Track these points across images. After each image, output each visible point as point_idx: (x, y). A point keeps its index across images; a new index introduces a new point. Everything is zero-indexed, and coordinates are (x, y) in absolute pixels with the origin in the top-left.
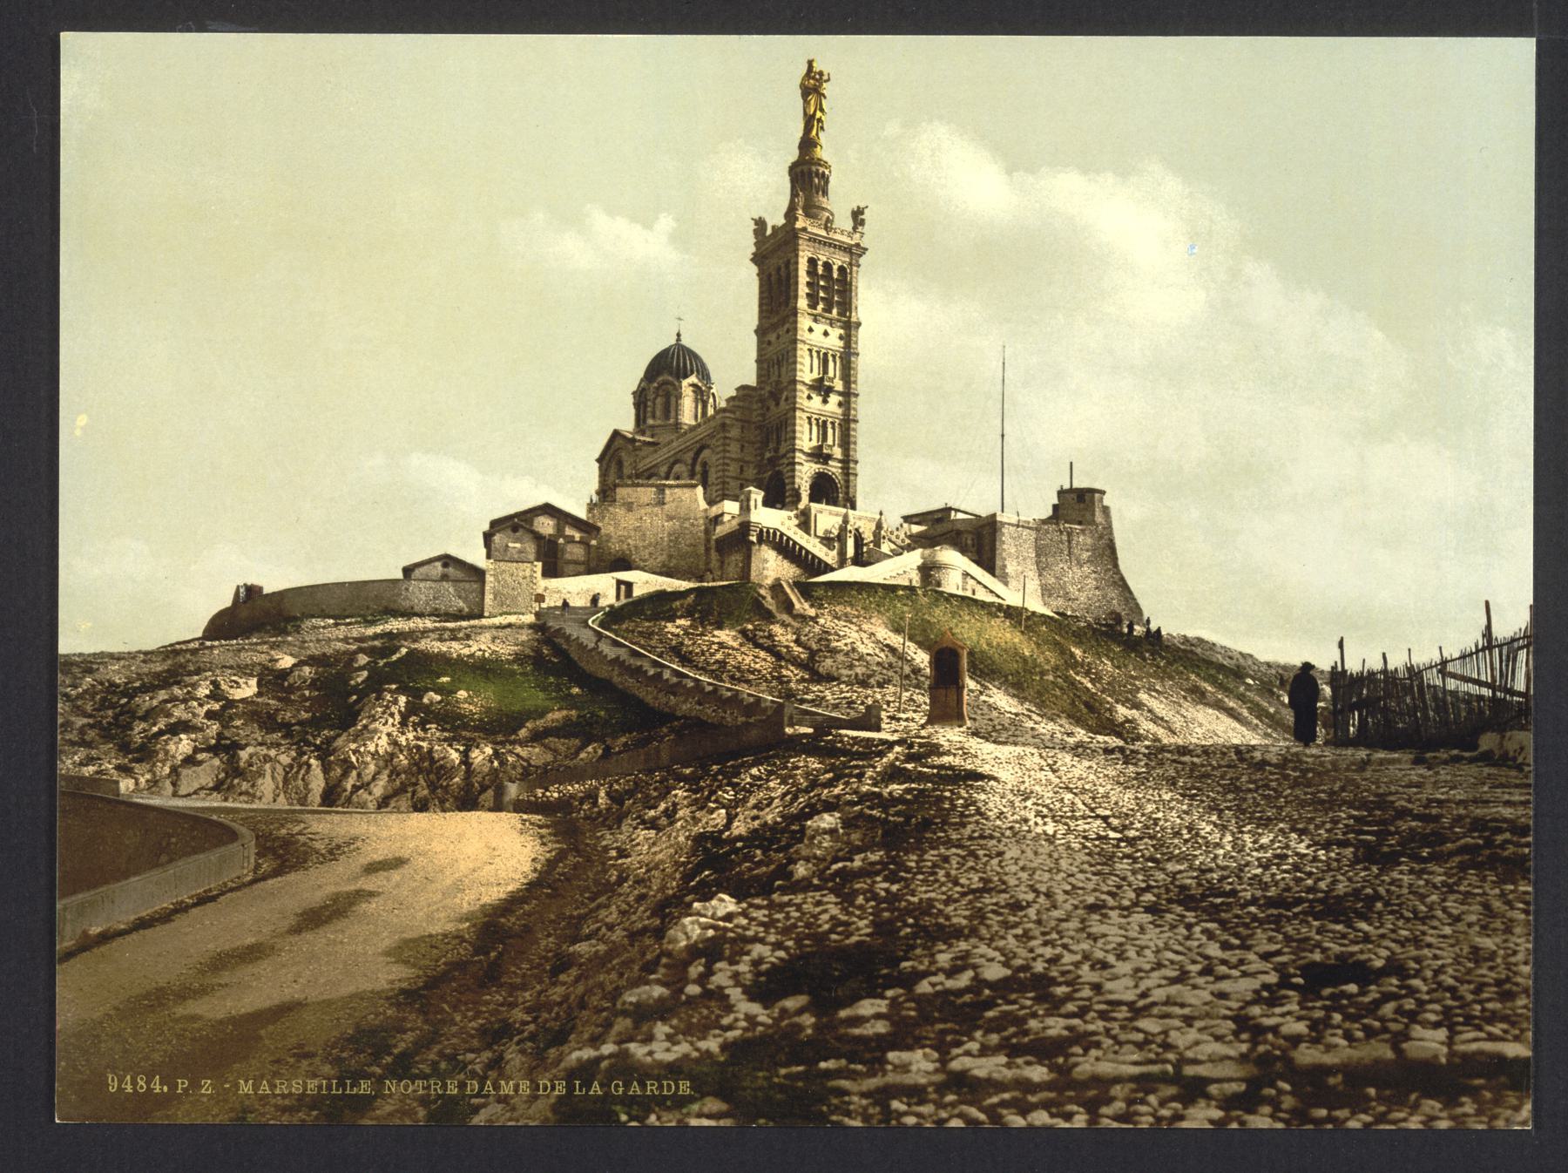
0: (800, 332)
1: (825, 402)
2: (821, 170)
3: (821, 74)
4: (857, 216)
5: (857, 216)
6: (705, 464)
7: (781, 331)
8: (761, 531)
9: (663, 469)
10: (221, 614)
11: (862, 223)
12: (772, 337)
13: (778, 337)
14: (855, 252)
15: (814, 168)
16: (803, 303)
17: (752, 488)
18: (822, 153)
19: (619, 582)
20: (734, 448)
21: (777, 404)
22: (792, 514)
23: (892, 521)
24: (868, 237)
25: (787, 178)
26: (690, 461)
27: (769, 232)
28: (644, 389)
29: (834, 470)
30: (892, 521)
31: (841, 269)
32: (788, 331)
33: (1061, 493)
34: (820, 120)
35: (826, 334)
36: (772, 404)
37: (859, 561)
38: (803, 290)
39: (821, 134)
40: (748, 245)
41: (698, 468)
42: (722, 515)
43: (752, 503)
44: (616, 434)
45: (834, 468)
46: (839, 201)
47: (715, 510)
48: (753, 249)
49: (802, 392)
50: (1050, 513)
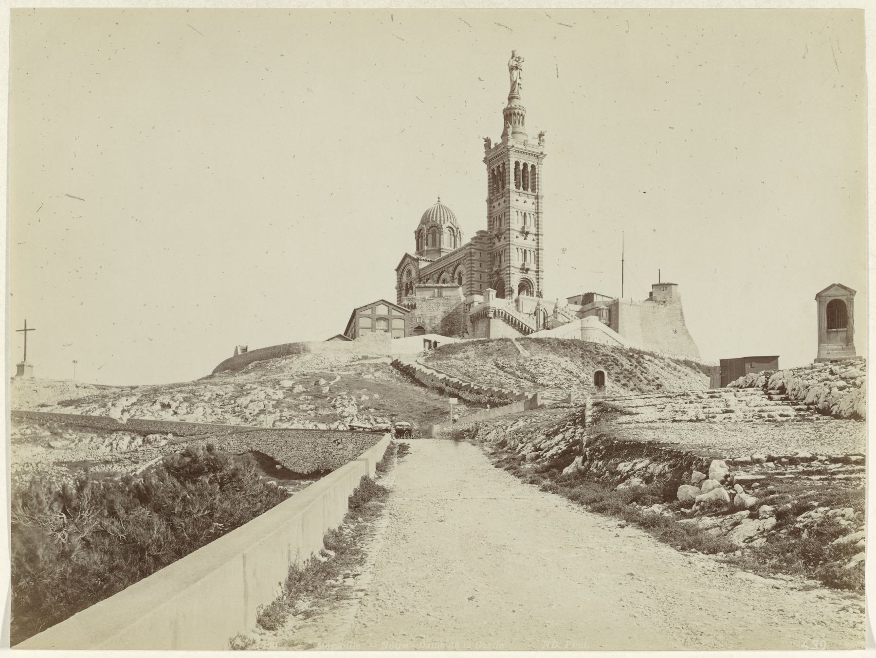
0: (511, 202)
6: (460, 274)
7: (501, 201)
8: (495, 311)
9: (435, 277)
10: (227, 361)
12: (496, 204)
13: (499, 204)
14: (539, 156)
15: (516, 111)
16: (512, 186)
17: (490, 289)
19: (425, 341)
20: (476, 265)
21: (499, 241)
22: (510, 301)
23: (563, 303)
24: (547, 148)
25: (502, 116)
26: (451, 271)
28: (421, 230)
29: (531, 276)
30: (563, 303)
31: (533, 167)
32: (505, 202)
35: (525, 202)
36: (496, 240)
37: (546, 327)
41: (456, 276)
42: (473, 302)
43: (490, 297)
44: (407, 256)
45: (531, 276)
47: (469, 300)
48: (484, 155)
49: (513, 234)
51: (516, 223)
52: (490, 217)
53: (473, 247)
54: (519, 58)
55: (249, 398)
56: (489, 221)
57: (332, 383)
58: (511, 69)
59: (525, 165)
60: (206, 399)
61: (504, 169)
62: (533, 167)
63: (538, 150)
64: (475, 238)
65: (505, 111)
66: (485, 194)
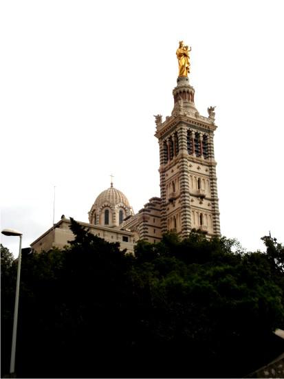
2: (190, 90)
3: (187, 47)
4: (211, 110)
5: (211, 110)
11: (214, 114)
12: (169, 172)
13: (173, 171)
21: (174, 206)
27: (164, 120)
28: (94, 210)
31: (205, 137)
34: (187, 68)
35: (198, 168)
39: (188, 75)
40: (153, 128)
46: (200, 106)
51: (192, 187)
52: (163, 185)
53: (146, 212)
54: (187, 47)
56: (162, 189)
58: (179, 56)
59: (197, 135)
61: (177, 141)
62: (205, 137)
63: (209, 122)
64: (148, 205)
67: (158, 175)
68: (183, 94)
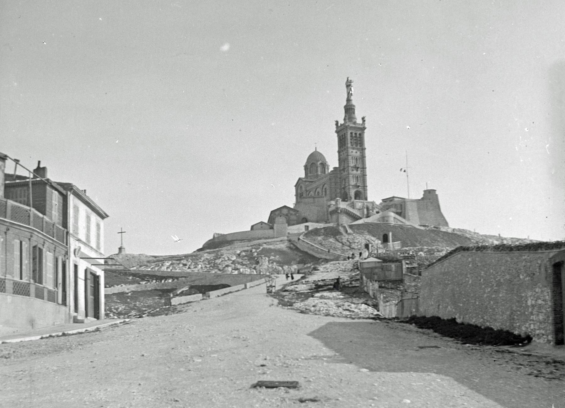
1: (357, 171)
3: (351, 81)
4: (363, 119)
5: (363, 119)
6: (325, 189)
7: (344, 152)
12: (342, 153)
13: (343, 154)
16: (349, 145)
18: (354, 102)
31: (360, 134)
33: (425, 191)
38: (349, 141)
40: (334, 128)
41: (324, 190)
42: (331, 205)
44: (300, 179)
45: (360, 189)
47: (329, 203)
50: (420, 196)
51: (352, 164)
54: (351, 81)
55: (220, 260)
56: (339, 162)
57: (258, 251)
59: (356, 134)
60: (202, 261)
61: (345, 137)
65: (345, 107)
66: (337, 149)
67: (337, 154)
68: (349, 109)
